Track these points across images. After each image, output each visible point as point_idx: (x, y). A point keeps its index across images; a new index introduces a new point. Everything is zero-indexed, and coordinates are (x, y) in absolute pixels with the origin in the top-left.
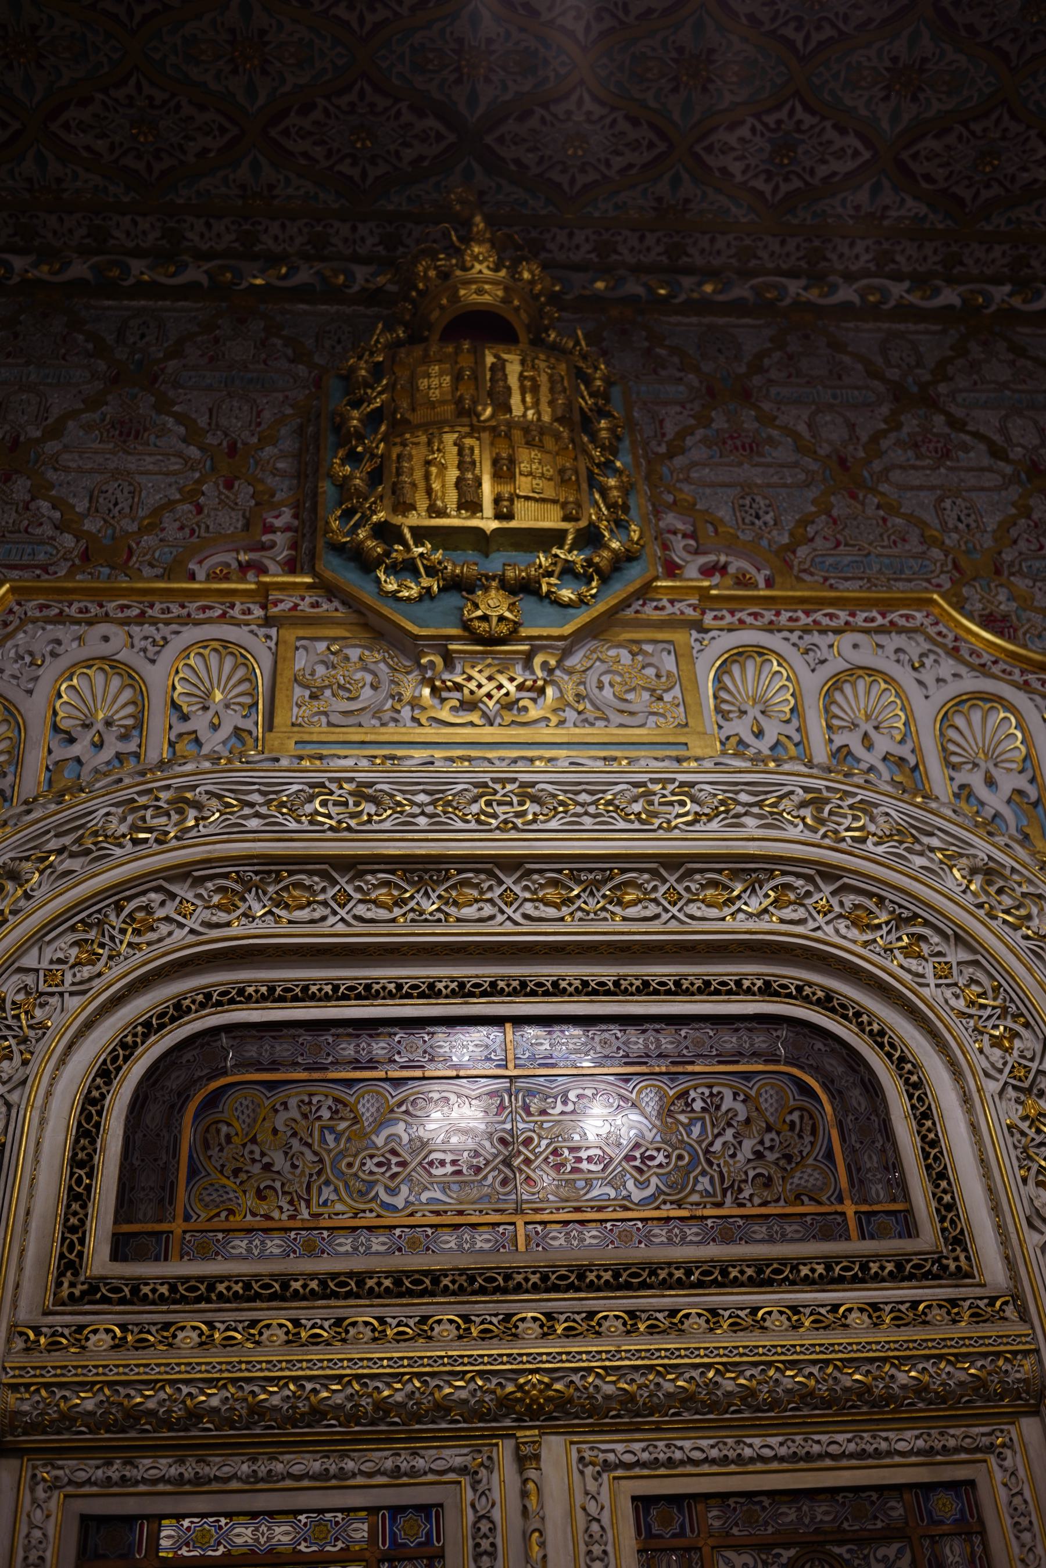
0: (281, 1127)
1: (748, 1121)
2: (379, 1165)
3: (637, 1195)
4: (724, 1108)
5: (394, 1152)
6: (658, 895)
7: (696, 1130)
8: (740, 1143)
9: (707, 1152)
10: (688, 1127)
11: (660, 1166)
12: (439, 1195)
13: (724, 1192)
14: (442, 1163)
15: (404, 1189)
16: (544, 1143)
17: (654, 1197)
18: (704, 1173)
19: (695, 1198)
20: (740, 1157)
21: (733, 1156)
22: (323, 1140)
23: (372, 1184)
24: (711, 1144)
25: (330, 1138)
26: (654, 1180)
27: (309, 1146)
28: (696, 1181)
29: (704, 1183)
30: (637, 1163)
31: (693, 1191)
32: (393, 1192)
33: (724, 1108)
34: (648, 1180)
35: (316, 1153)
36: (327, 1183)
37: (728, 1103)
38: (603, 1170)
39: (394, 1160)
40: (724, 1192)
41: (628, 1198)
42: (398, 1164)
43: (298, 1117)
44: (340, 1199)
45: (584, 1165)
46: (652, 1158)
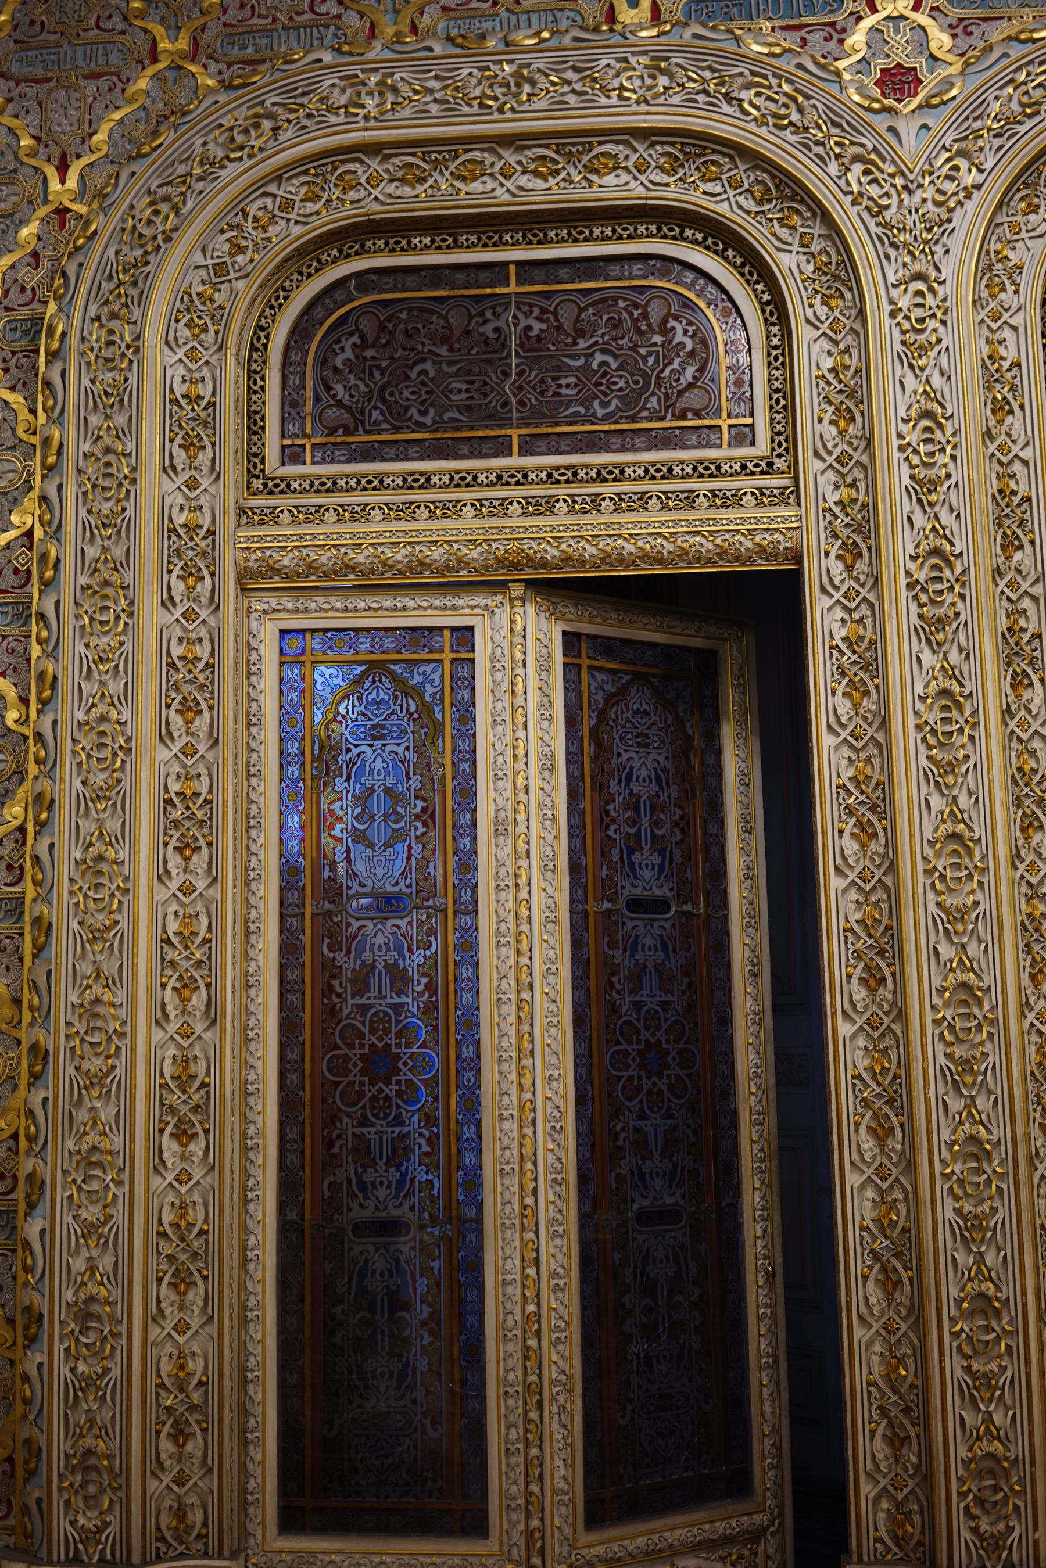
0: (339, 365)
1: (692, 353)
2: (413, 393)
3: (600, 412)
4: (674, 343)
5: (423, 383)
6: (630, 163)
7: (651, 361)
8: (684, 369)
9: (658, 377)
10: (645, 359)
11: (621, 390)
12: (457, 415)
13: (667, 408)
14: (460, 391)
15: (432, 412)
16: (533, 374)
17: (612, 414)
18: (653, 394)
19: (645, 414)
20: (683, 381)
21: (678, 380)
22: (371, 374)
23: (407, 408)
24: (662, 371)
25: (377, 375)
26: (615, 402)
27: (363, 380)
28: (647, 400)
29: (653, 402)
30: (603, 388)
31: (643, 408)
32: (424, 413)
33: (674, 343)
34: (610, 402)
35: (367, 386)
36: (376, 408)
37: (679, 337)
38: (578, 393)
39: (424, 389)
40: (667, 408)
41: (594, 415)
42: (426, 393)
43: (353, 359)
44: (386, 421)
45: (563, 391)
46: (615, 383)
